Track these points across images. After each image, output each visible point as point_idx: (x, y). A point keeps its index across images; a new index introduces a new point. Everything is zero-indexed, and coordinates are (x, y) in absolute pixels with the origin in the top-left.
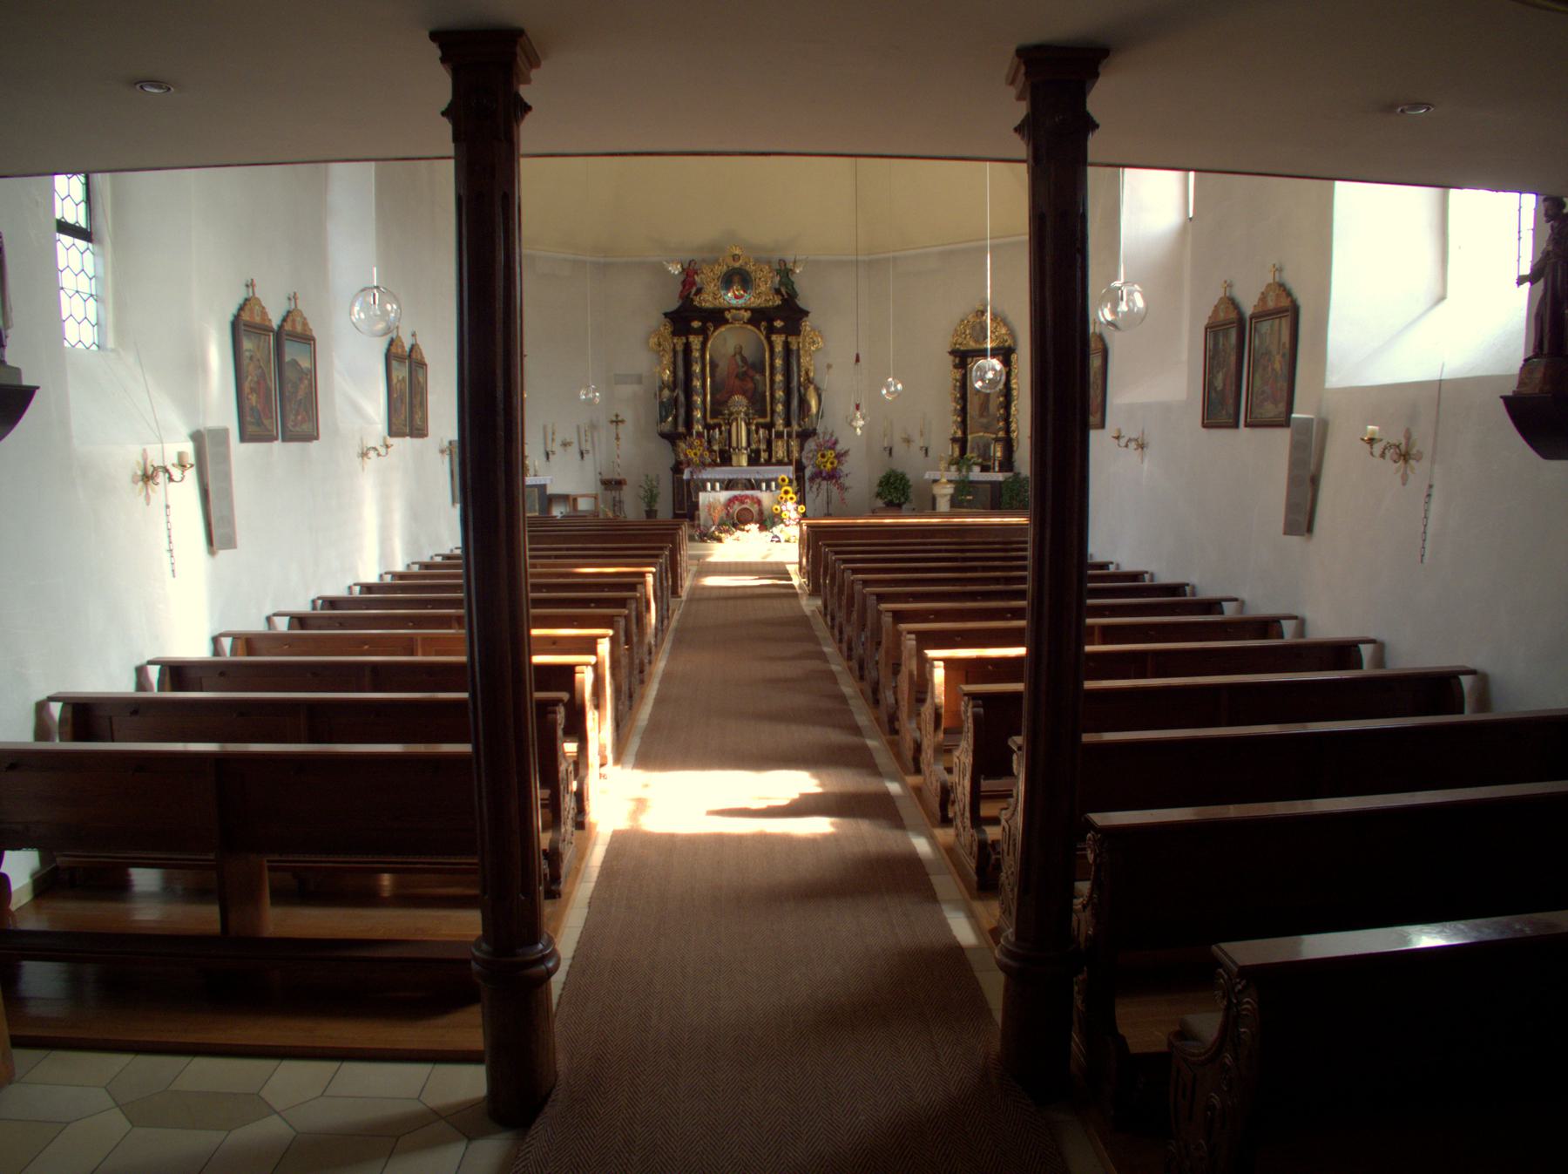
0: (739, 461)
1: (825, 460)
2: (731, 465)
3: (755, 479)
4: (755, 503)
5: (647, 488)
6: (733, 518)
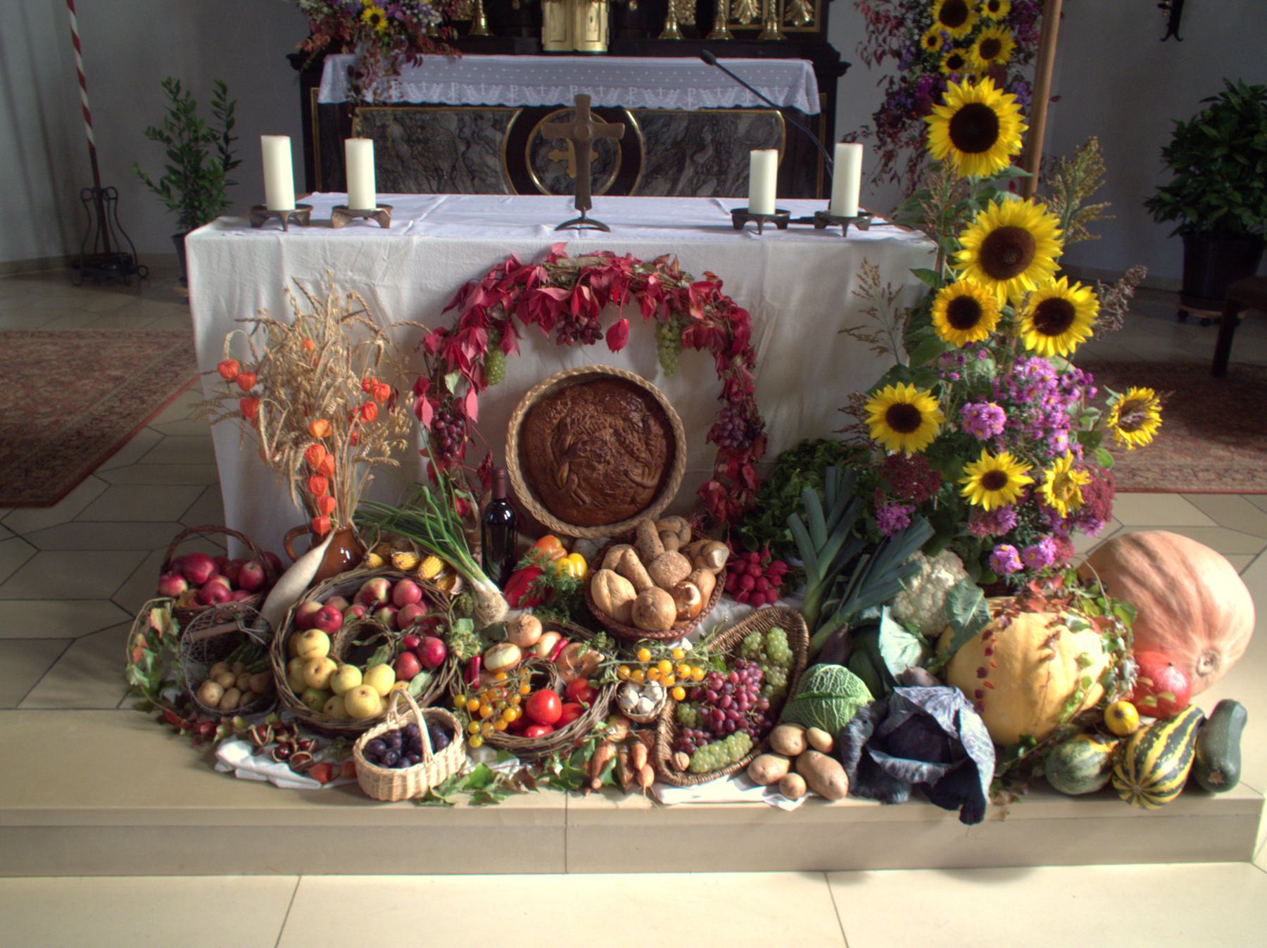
0: (569, 30)
1: (964, 31)
2: (541, 51)
3: (641, 113)
4: (698, 339)
5: (178, 144)
6: (489, 476)
